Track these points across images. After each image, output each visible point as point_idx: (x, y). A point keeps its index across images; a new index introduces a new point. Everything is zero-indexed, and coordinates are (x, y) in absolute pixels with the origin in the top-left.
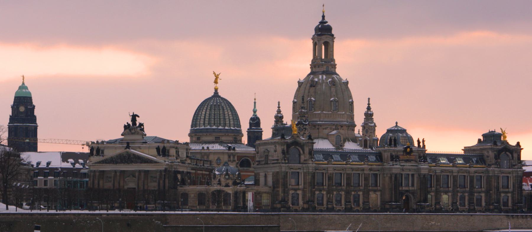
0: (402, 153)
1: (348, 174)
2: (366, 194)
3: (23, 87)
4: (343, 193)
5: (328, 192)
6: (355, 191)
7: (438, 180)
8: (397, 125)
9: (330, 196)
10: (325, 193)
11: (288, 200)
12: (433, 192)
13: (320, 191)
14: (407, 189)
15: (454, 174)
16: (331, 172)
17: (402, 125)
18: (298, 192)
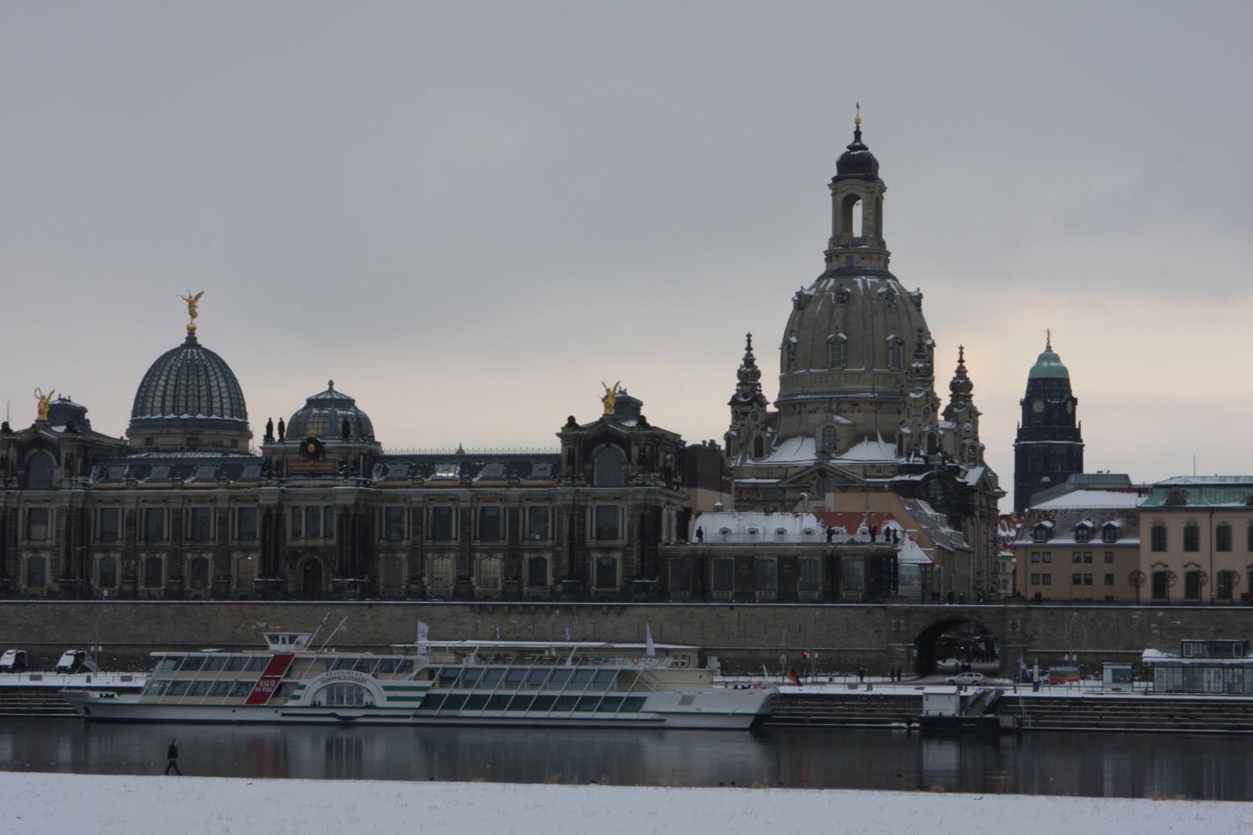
0: (297, 456)
1: (175, 511)
2: (224, 557)
3: (1049, 356)
4: (164, 556)
5: (126, 556)
6: (193, 551)
7: (417, 520)
8: (331, 389)
9: (129, 564)
10: (118, 556)
11: (17, 573)
12: (403, 550)
13: (107, 551)
14: (311, 543)
15: (462, 505)
16: (133, 506)
17: (343, 388)
18: (42, 555)
